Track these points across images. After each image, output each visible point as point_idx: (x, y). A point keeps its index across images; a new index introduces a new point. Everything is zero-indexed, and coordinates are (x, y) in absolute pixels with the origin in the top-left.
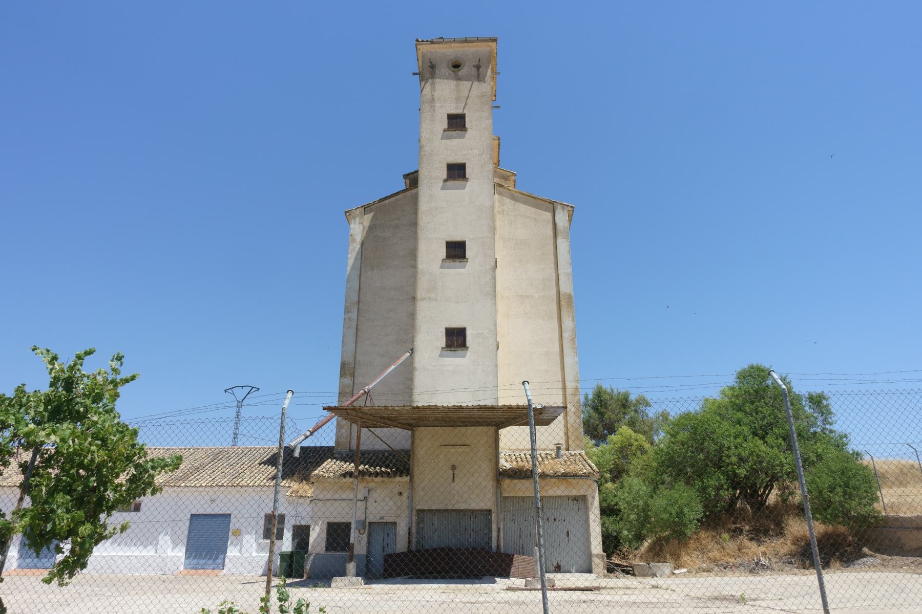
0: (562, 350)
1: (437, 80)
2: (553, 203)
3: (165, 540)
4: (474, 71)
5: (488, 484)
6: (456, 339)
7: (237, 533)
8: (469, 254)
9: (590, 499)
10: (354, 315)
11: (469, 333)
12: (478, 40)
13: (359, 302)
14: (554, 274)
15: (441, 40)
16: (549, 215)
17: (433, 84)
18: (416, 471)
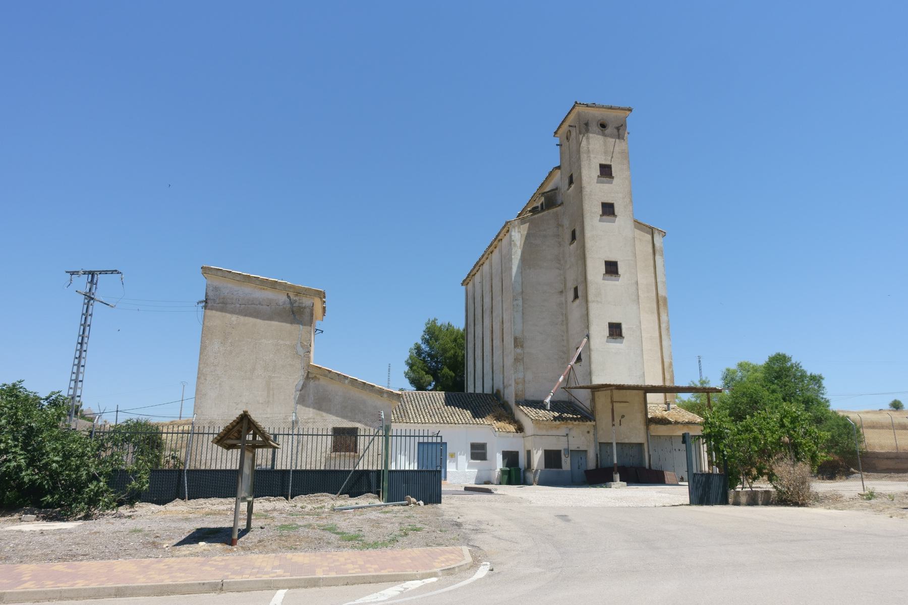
1: (591, 135)
2: (652, 229)
4: (616, 131)
5: (642, 427)
6: (615, 330)
7: (453, 455)
8: (620, 271)
10: (520, 302)
11: (624, 327)
12: (619, 109)
13: (522, 292)
14: (654, 281)
15: (594, 106)
16: (649, 237)
17: (588, 138)
18: (597, 418)
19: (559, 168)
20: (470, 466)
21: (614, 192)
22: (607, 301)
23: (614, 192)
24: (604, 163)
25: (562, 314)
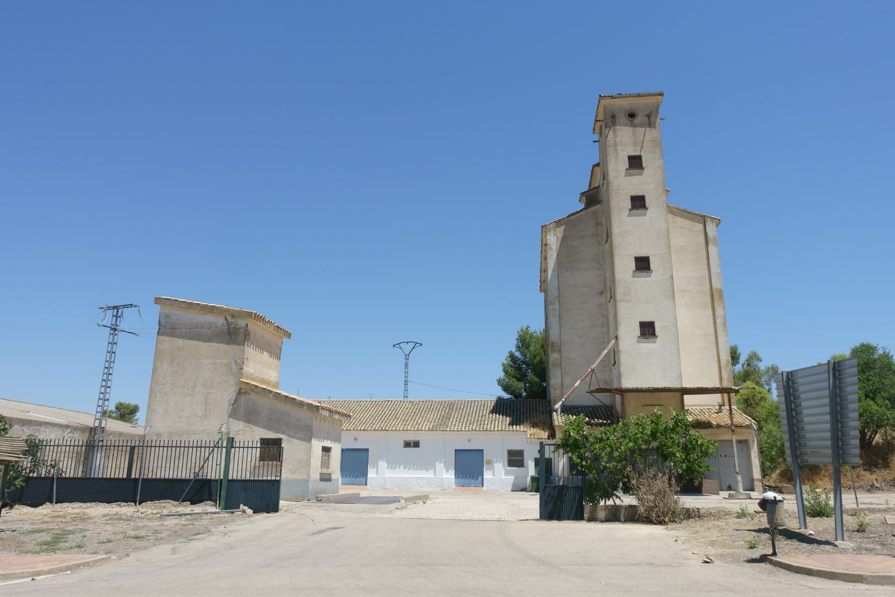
0: (716, 332)
2: (704, 217)
3: (440, 466)
6: (648, 330)
7: (490, 462)
8: (652, 266)
9: (751, 442)
11: (657, 325)
12: (649, 95)
15: (620, 96)
16: (701, 226)
17: (615, 131)
19: (598, 165)
20: (507, 473)
21: (645, 183)
22: (636, 299)
23: (645, 183)
24: (632, 154)
25: (603, 315)
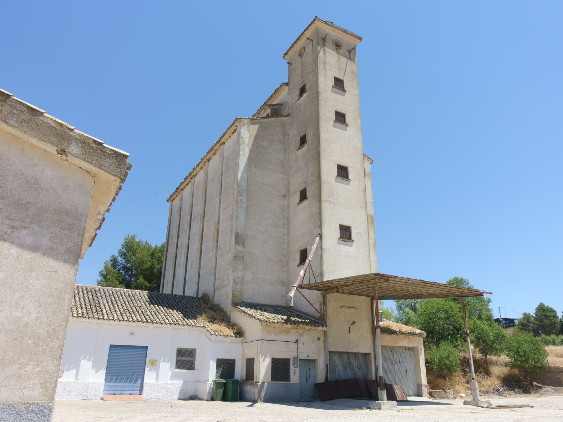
3: (86, 365)
7: (154, 363)
8: (351, 176)
9: (419, 348)
10: (244, 198)
11: (353, 231)
12: (352, 34)
13: (247, 189)
15: (331, 24)
19: (287, 84)
20: (174, 377)
21: (347, 103)
23: (347, 103)
24: (338, 76)
25: (284, 217)
